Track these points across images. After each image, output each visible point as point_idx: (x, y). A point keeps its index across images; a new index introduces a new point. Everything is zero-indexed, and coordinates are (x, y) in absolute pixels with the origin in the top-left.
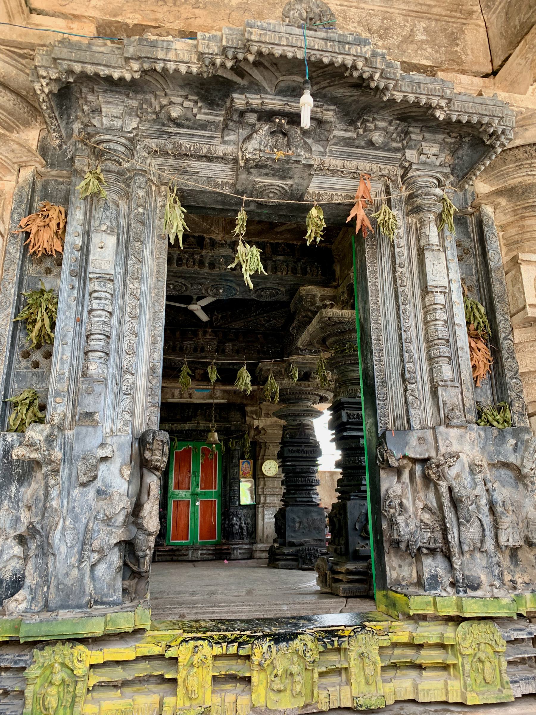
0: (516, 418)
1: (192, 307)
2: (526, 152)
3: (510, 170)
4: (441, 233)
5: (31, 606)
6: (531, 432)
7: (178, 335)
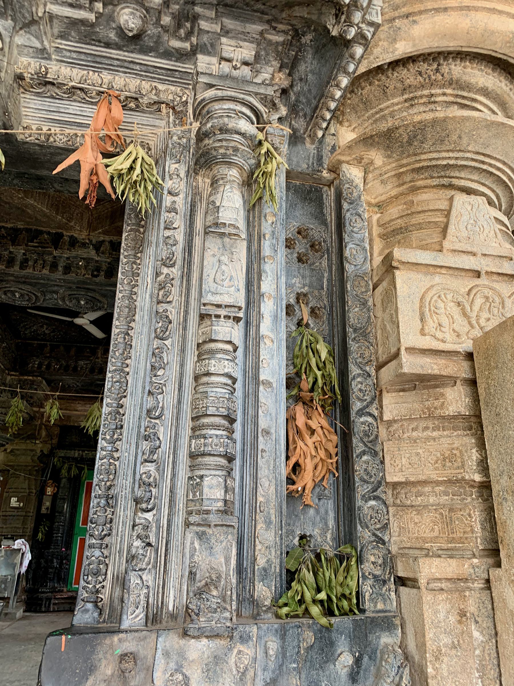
0: (367, 589)
1: (78, 321)
2: (420, 73)
3: (396, 108)
4: (253, 208)
6: (395, 627)
7: (72, 352)
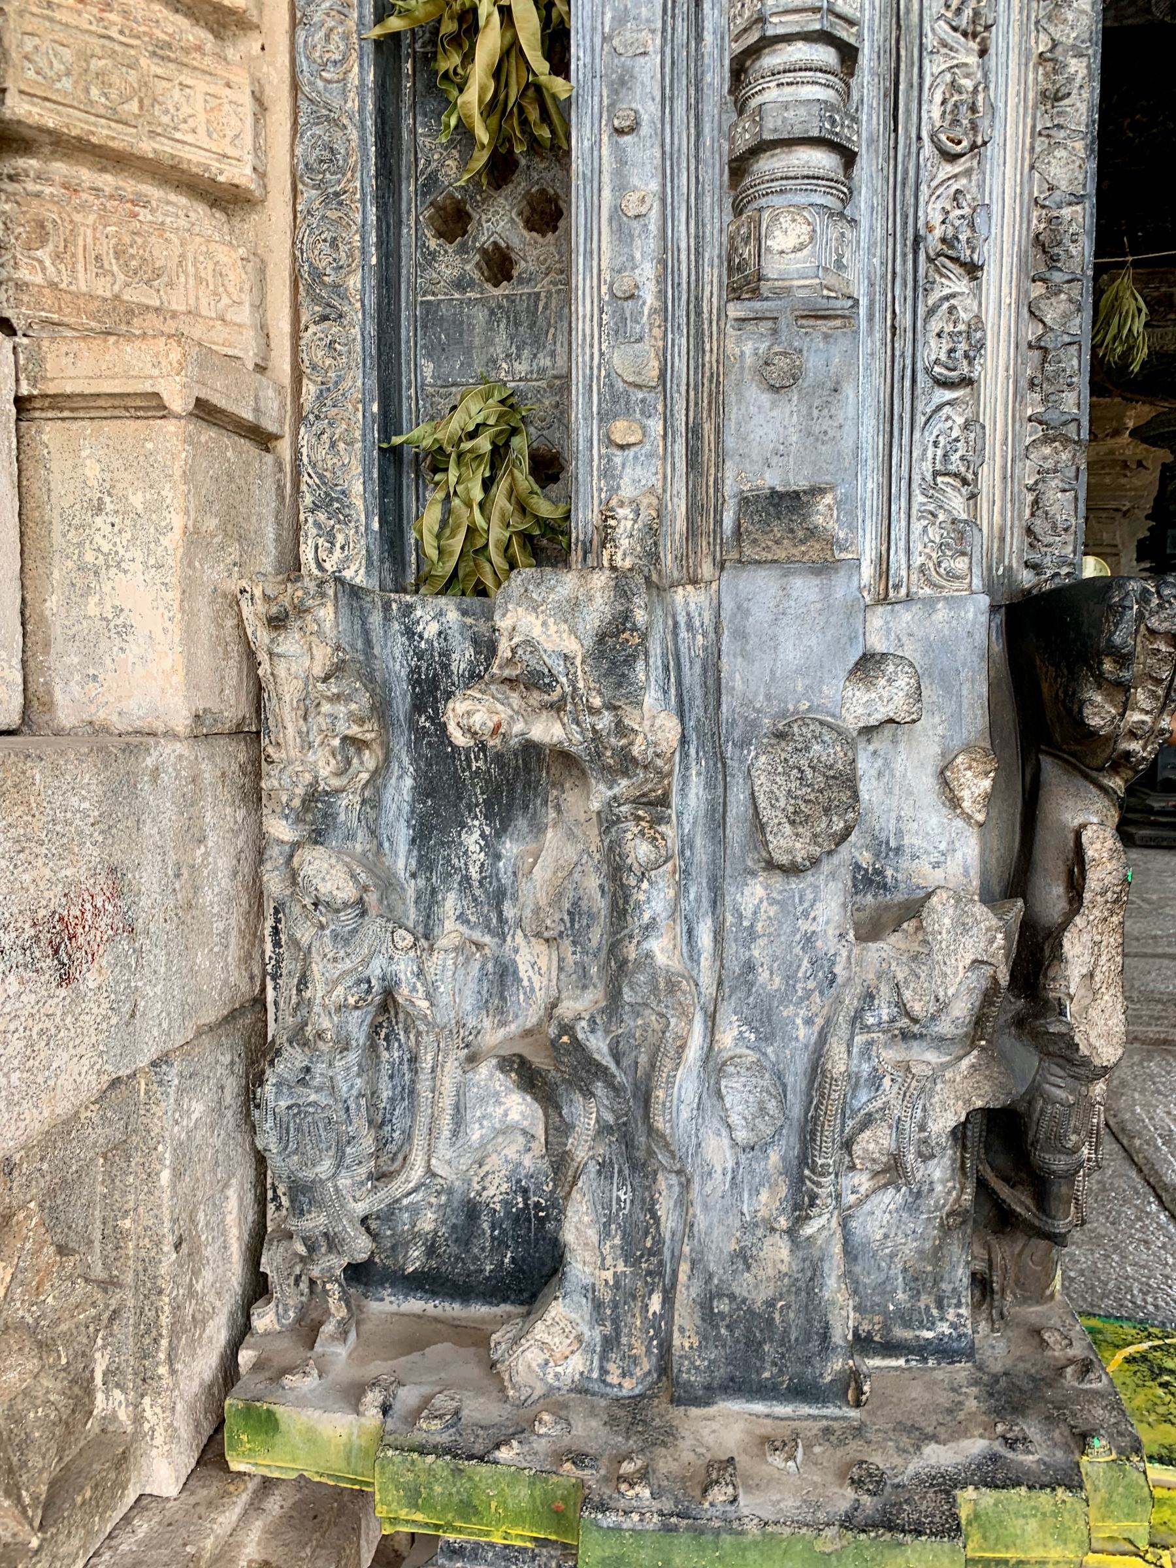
5: (604, 1371)
